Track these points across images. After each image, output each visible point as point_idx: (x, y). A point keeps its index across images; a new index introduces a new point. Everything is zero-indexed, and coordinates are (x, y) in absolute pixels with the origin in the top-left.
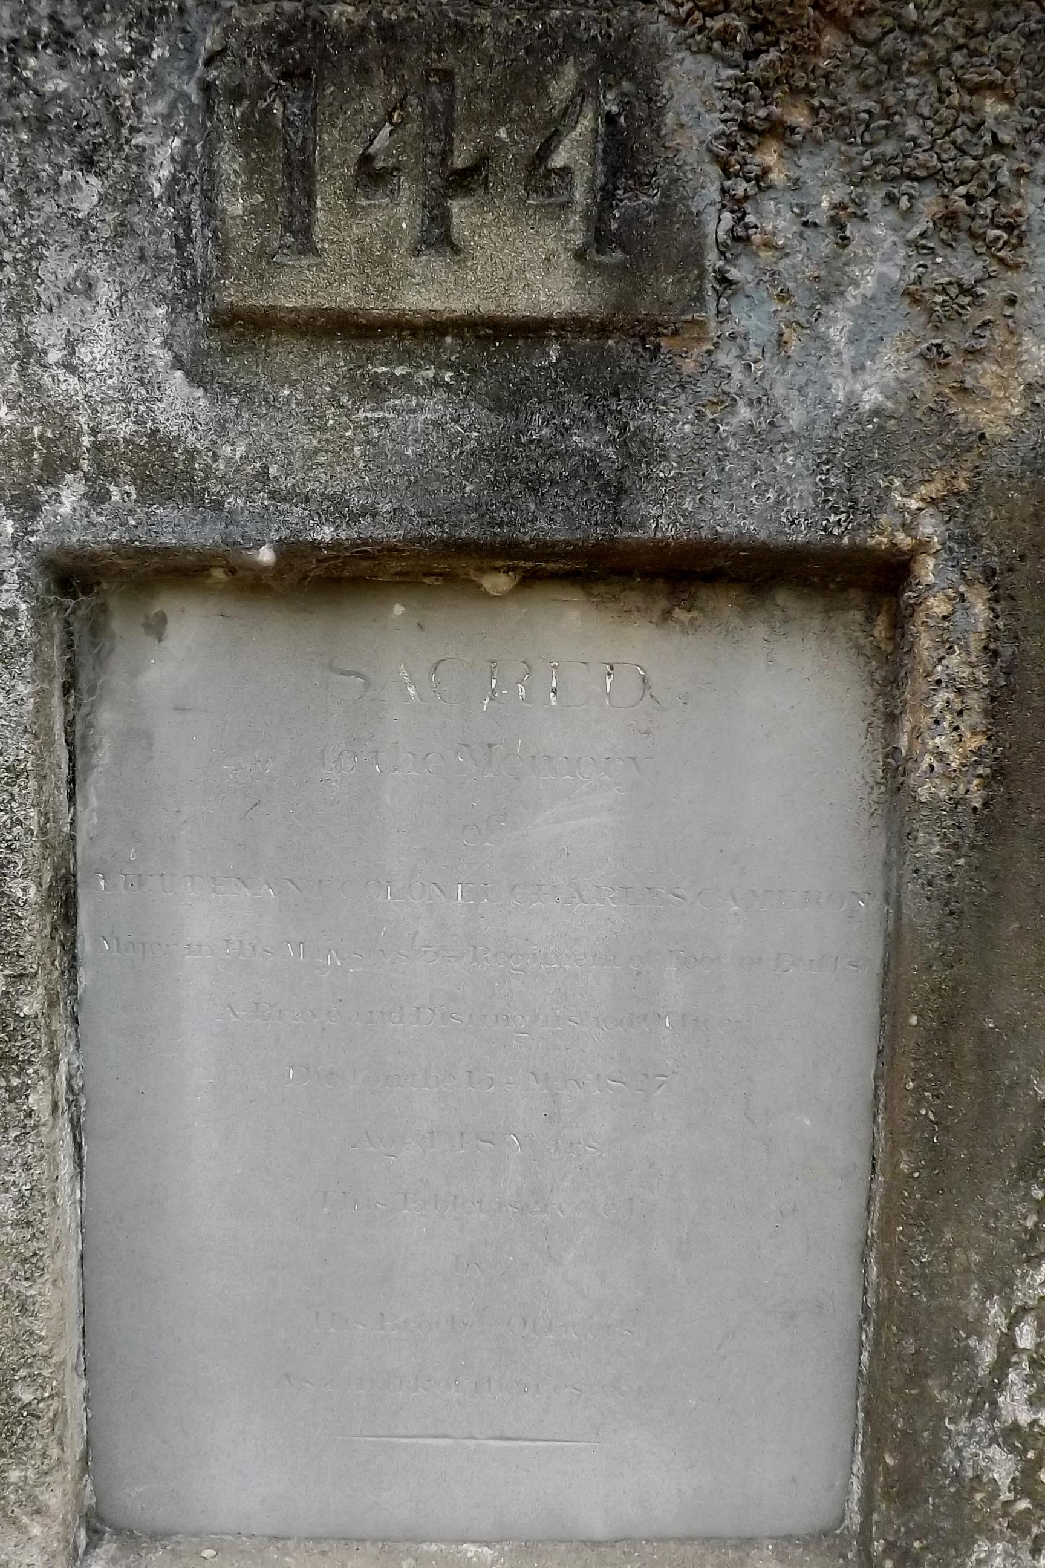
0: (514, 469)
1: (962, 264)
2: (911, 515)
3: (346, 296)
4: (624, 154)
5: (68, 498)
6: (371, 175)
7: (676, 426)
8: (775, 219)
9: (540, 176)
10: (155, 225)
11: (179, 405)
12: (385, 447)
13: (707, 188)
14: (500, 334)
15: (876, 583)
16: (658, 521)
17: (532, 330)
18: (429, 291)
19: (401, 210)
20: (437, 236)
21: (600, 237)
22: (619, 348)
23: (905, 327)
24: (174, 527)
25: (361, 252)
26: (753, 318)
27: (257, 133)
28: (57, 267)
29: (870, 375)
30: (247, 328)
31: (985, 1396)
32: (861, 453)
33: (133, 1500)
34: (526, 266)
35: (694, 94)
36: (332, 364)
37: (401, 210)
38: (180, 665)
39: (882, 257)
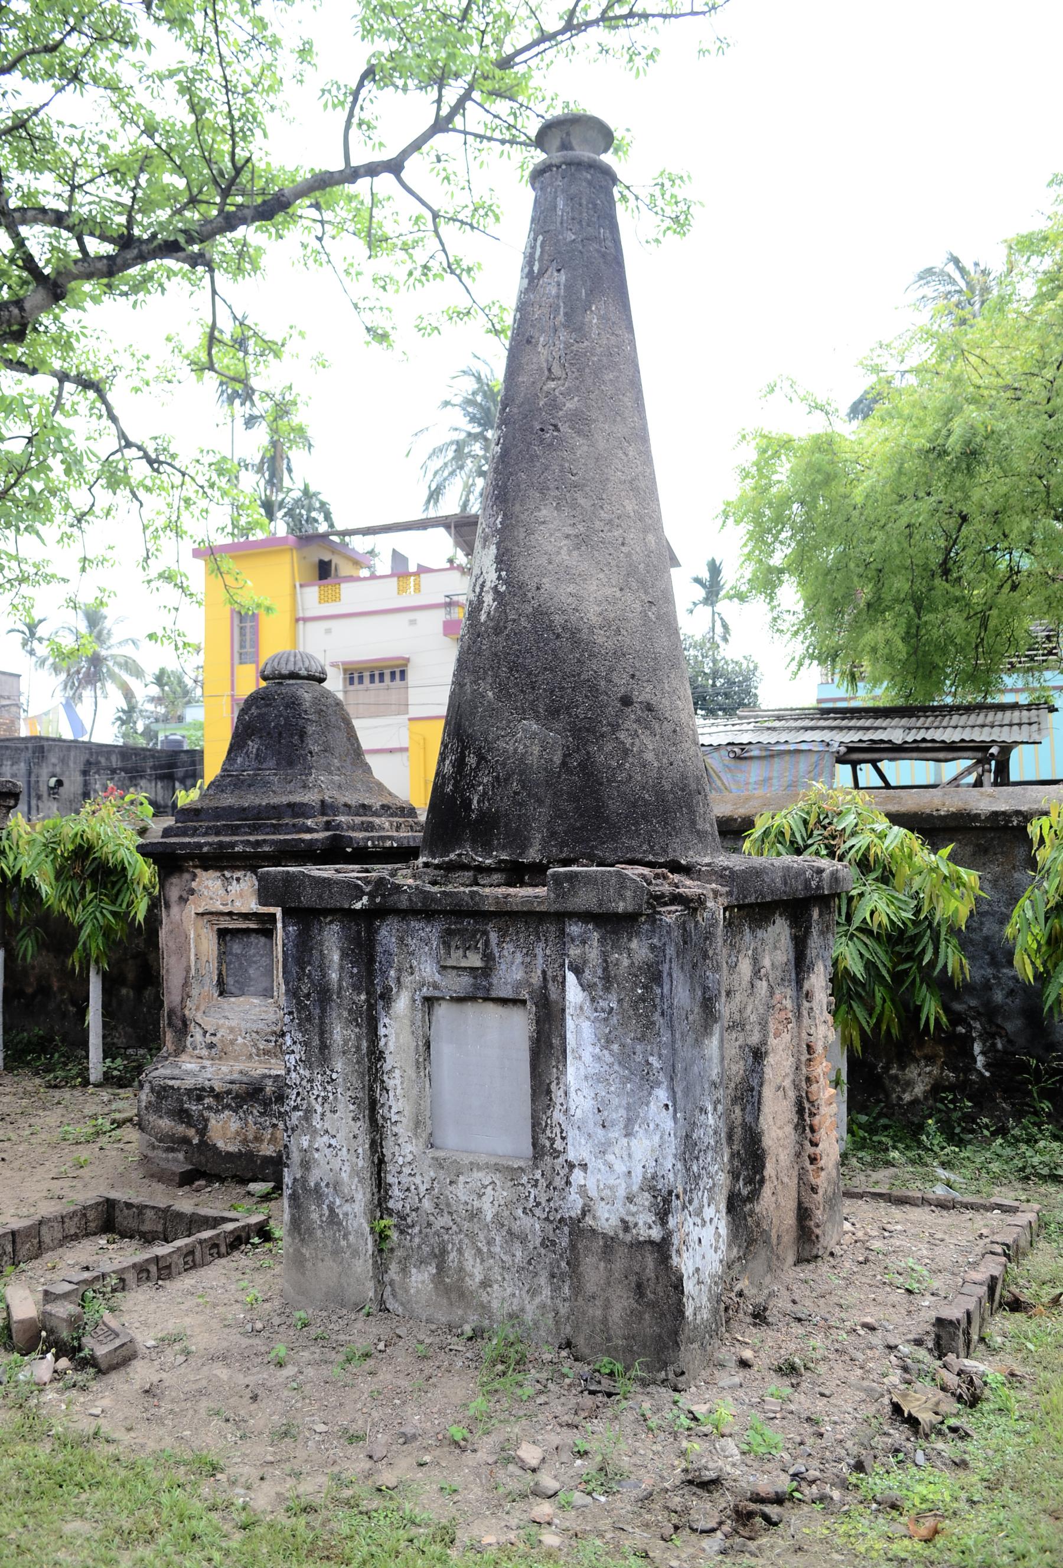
0: (476, 987)
1: (528, 959)
2: (525, 995)
3: (455, 964)
4: (487, 944)
5: (425, 989)
6: (457, 948)
7: (495, 981)
8: (505, 953)
9: (476, 948)
10: (434, 953)
11: (437, 977)
12: (461, 983)
13: (496, 950)
14: (473, 969)
15: (523, 1002)
16: (494, 994)
17: (477, 969)
18: (464, 963)
19: (460, 952)
20: (465, 956)
21: (484, 955)
22: (486, 971)
23: (522, 968)
24: (437, 994)
25: (456, 958)
26: (503, 967)
27: (444, 943)
28: (423, 959)
29: (518, 975)
30: (444, 968)
31: (544, 1131)
32: (518, 985)
33: (438, 1142)
34: (475, 960)
35: (493, 937)
36: (455, 972)
37: (460, 952)
38: (442, 1010)
39: (519, 958)
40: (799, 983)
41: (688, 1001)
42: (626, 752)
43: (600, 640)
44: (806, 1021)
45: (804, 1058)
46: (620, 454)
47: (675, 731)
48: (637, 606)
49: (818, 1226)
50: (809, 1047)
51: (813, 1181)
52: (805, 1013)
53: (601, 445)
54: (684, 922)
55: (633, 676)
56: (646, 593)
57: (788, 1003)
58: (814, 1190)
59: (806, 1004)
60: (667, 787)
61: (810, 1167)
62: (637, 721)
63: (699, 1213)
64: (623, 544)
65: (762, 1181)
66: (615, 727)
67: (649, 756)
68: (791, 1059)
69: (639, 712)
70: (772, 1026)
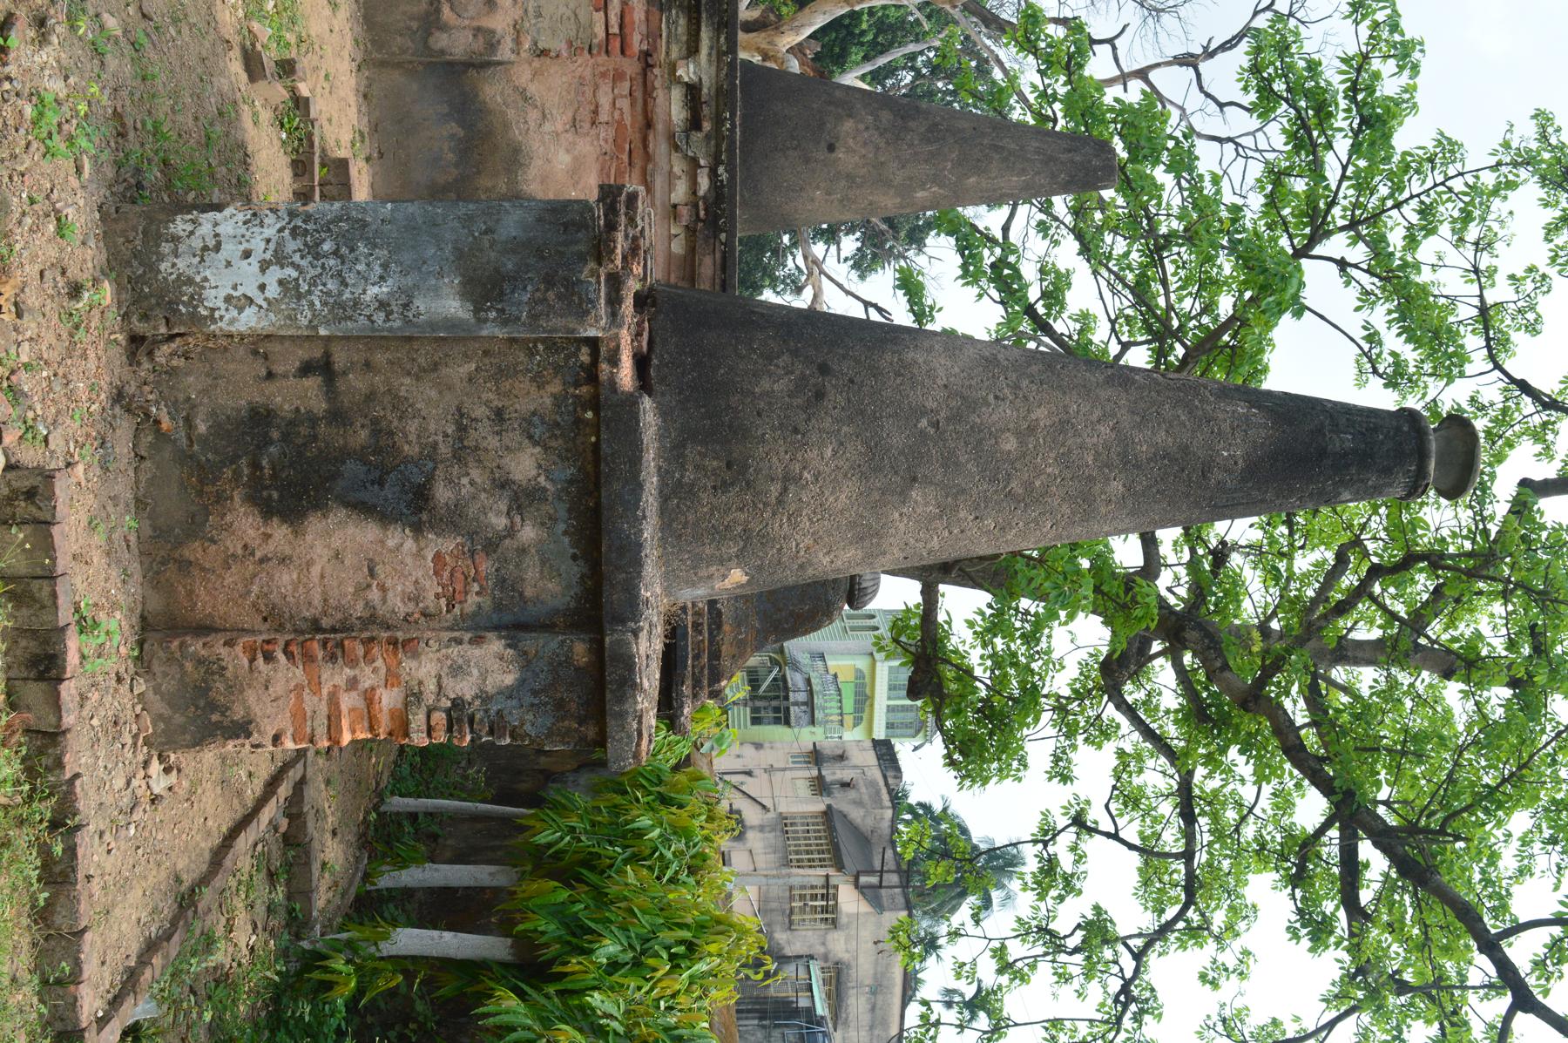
40: (496, 628)
41: (503, 238)
42: (770, 358)
43: (888, 356)
44: (446, 635)
45: (400, 635)
46: (1097, 413)
47: (796, 431)
48: (931, 404)
49: (182, 645)
50: (411, 640)
51: (241, 642)
52: (456, 634)
53: (1104, 394)
54: (586, 227)
55: (851, 381)
56: (948, 419)
57: (472, 600)
58: (229, 643)
59: (467, 636)
60: (734, 400)
61: (260, 639)
62: (803, 377)
63: (280, 259)
64: (996, 397)
65: (268, 511)
66: (795, 353)
67: (766, 384)
68: (402, 609)
69: (812, 381)
70: (448, 544)
